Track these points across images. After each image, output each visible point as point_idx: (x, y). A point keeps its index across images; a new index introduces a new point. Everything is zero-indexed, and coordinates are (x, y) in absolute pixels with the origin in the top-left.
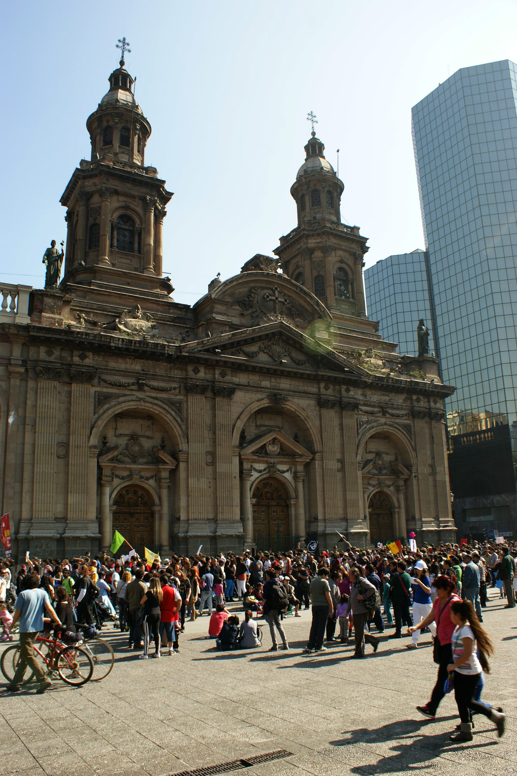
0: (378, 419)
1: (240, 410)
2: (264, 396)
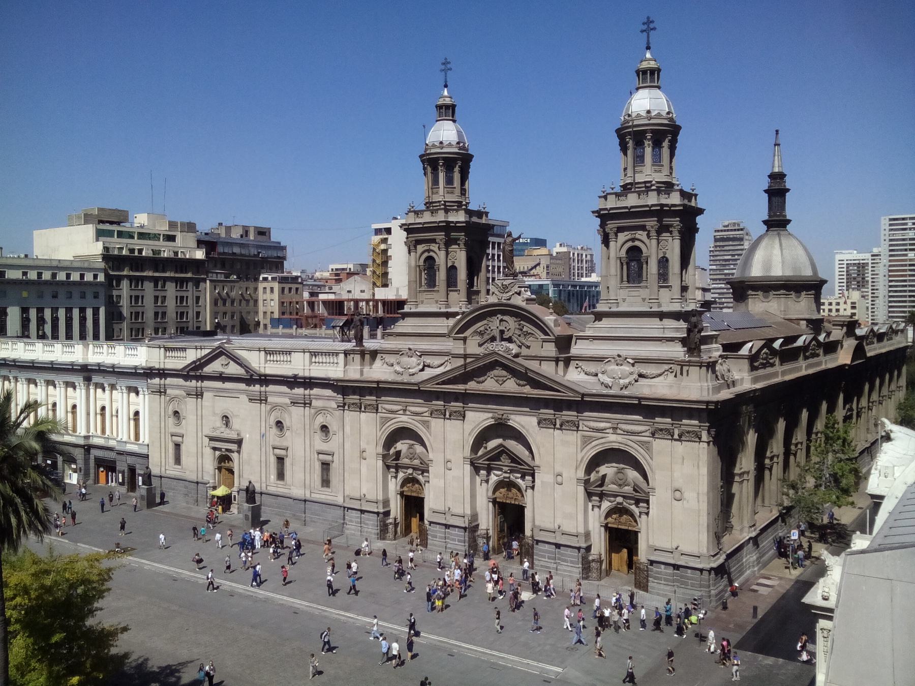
0: (607, 435)
1: (472, 427)
2: (490, 415)
